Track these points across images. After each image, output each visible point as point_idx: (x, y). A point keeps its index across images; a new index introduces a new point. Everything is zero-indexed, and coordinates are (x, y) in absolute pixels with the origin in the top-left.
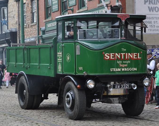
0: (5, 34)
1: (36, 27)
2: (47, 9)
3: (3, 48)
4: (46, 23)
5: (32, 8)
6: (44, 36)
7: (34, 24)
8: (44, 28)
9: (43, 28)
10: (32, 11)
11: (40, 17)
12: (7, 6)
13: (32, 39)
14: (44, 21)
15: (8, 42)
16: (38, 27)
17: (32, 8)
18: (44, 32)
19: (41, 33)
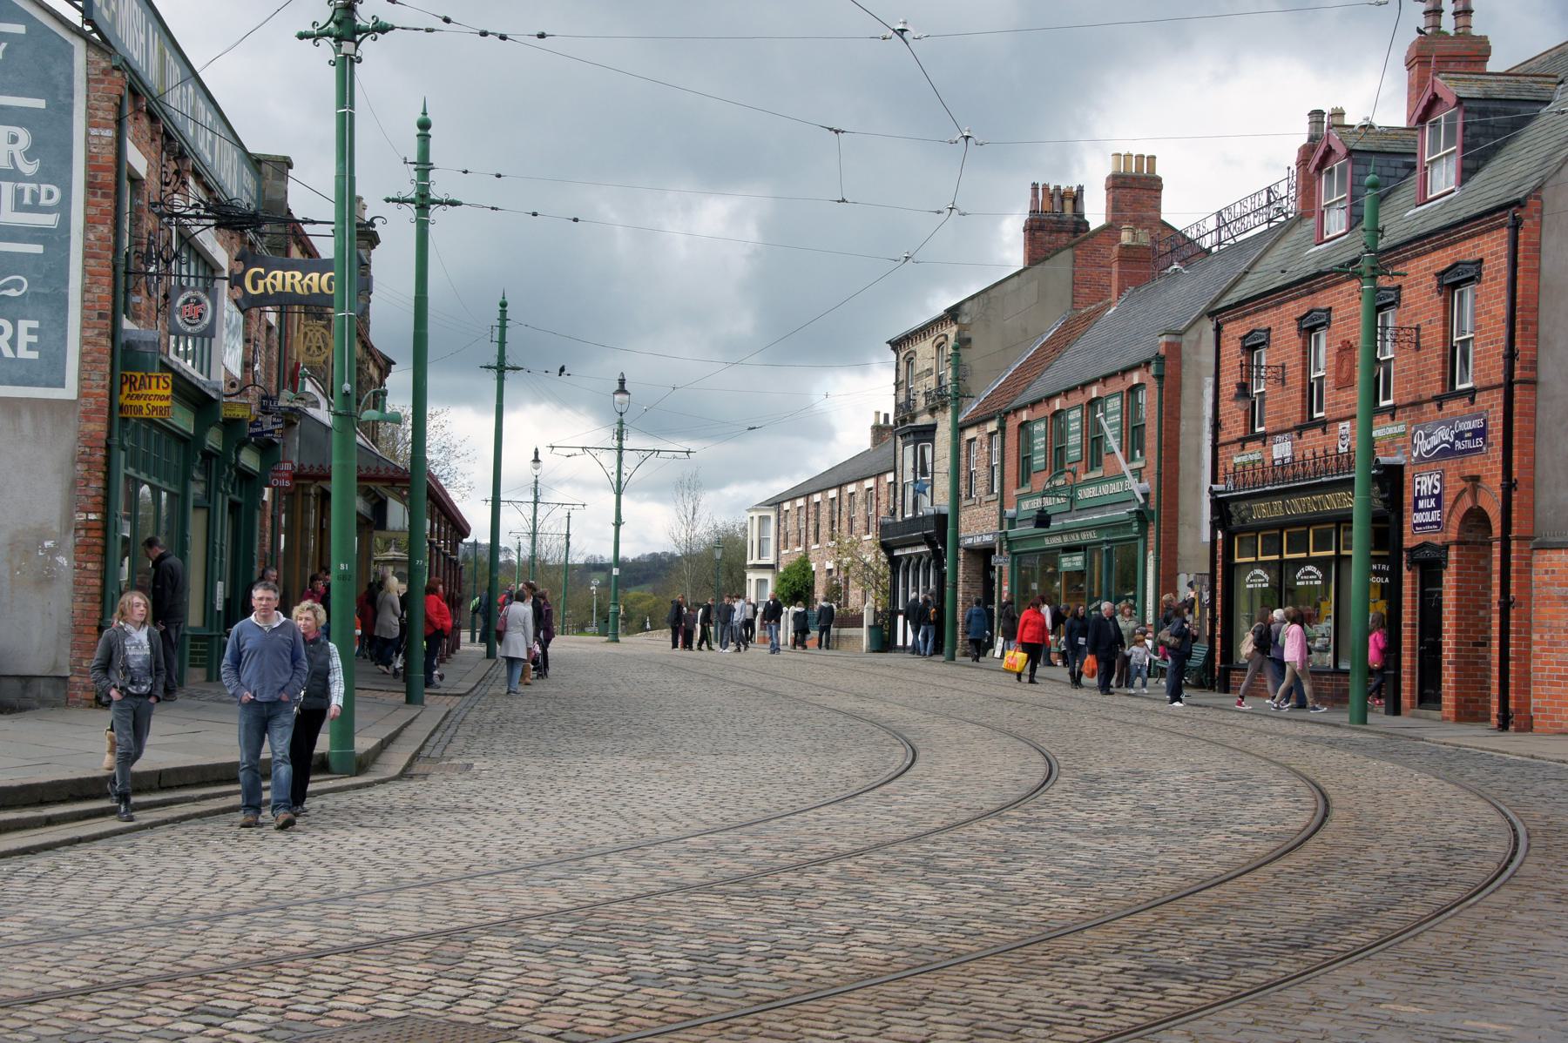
0: (924, 518)
1: (996, 505)
2: (1025, 463)
3: (920, 556)
4: (1021, 498)
5: (990, 453)
6: (1012, 533)
7: (993, 497)
8: (1014, 511)
9: (1011, 511)
10: (990, 461)
11: (1006, 480)
12: (932, 441)
13: (988, 538)
14: (1015, 492)
15: (928, 540)
16: (1002, 507)
17: (990, 453)
18: (1012, 522)
19: (1006, 523)
